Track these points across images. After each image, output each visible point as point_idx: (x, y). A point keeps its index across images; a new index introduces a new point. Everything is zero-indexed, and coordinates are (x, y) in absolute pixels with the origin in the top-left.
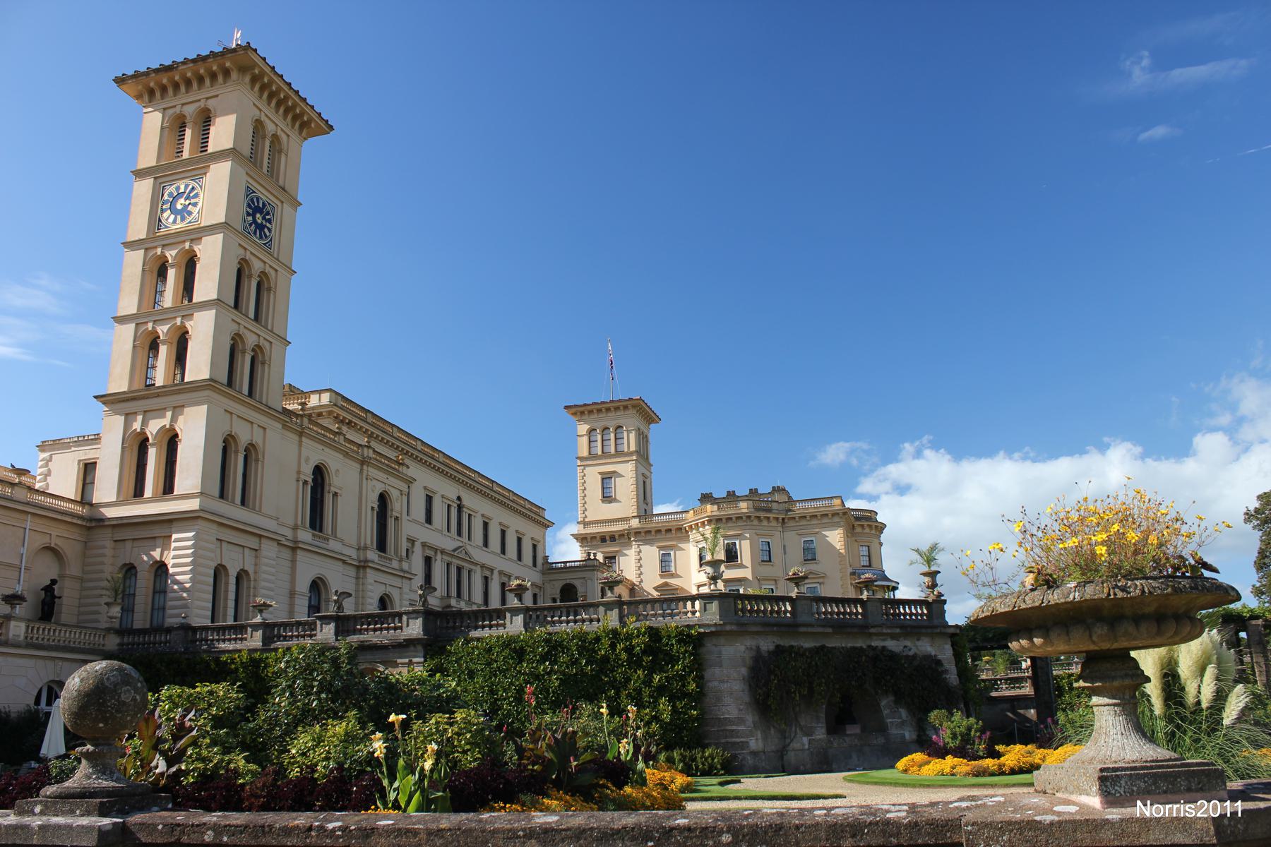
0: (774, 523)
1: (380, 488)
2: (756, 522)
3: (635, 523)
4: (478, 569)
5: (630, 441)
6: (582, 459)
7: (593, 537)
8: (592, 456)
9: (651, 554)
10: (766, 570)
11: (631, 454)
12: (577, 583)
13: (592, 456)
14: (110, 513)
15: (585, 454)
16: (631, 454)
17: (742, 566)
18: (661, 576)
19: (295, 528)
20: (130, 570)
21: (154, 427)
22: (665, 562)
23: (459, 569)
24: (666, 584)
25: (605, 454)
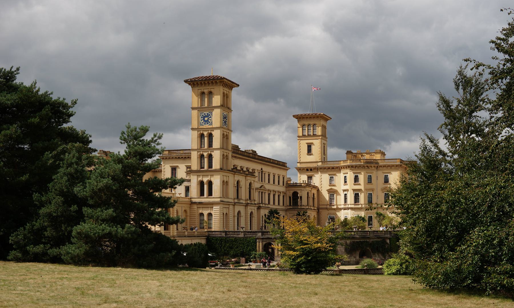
0: (374, 168)
1: (249, 181)
2: (366, 168)
3: (320, 164)
4: (267, 192)
5: (319, 131)
6: (299, 137)
7: (303, 169)
8: (304, 136)
9: (326, 177)
10: (370, 186)
11: (319, 136)
12: (299, 191)
13: (304, 136)
14: (194, 200)
15: (301, 135)
16: (319, 136)
17: (359, 184)
18: (330, 186)
19: (234, 199)
20: (202, 214)
21: (205, 180)
22: (331, 179)
23: (262, 193)
24: (331, 189)
25: (309, 135)
